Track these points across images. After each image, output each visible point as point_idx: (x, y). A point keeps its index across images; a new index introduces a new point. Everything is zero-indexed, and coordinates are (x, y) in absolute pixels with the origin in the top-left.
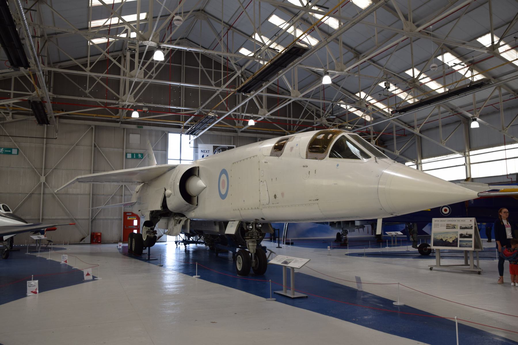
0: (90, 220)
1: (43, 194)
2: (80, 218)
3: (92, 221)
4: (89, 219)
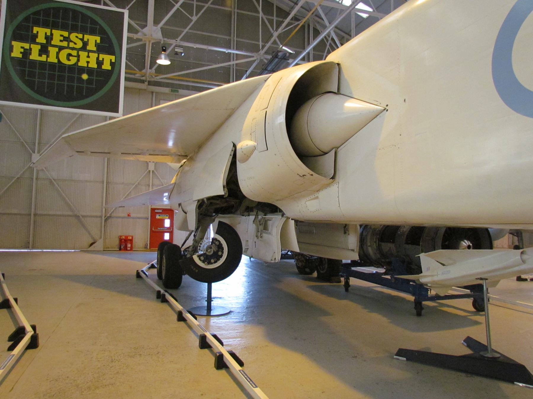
0: (103, 219)
1: (37, 179)
2: (89, 214)
3: (106, 221)
4: (101, 217)
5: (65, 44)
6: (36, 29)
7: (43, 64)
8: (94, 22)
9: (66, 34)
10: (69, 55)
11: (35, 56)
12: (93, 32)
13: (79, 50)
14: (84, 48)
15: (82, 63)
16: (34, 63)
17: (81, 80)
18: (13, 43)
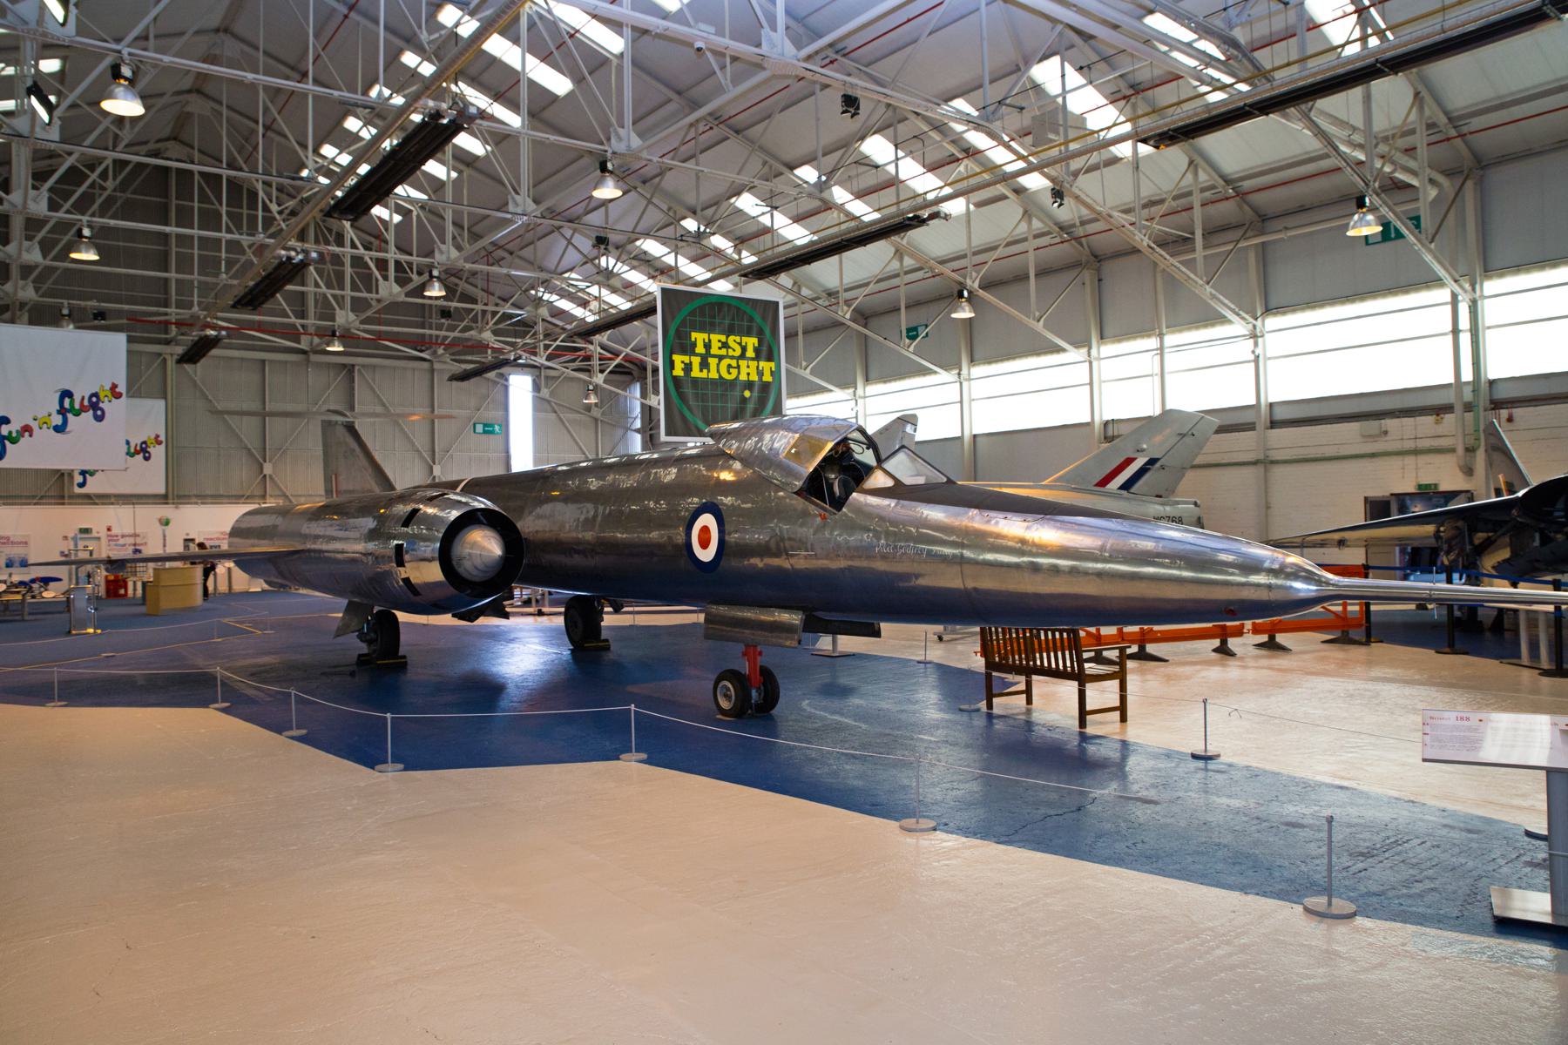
5: (723, 352)
6: (694, 335)
7: (706, 381)
8: (751, 319)
9: (723, 338)
10: (729, 366)
11: (696, 373)
12: (749, 334)
13: (738, 358)
14: (743, 356)
15: (743, 377)
16: (695, 381)
17: (744, 400)
18: (675, 357)
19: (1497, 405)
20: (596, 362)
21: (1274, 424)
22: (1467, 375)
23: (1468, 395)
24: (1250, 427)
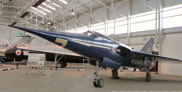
19: (164, 34)
20: (37, 23)
21: (131, 37)
22: (158, 28)
23: (158, 33)
24: (126, 38)
